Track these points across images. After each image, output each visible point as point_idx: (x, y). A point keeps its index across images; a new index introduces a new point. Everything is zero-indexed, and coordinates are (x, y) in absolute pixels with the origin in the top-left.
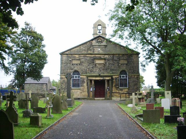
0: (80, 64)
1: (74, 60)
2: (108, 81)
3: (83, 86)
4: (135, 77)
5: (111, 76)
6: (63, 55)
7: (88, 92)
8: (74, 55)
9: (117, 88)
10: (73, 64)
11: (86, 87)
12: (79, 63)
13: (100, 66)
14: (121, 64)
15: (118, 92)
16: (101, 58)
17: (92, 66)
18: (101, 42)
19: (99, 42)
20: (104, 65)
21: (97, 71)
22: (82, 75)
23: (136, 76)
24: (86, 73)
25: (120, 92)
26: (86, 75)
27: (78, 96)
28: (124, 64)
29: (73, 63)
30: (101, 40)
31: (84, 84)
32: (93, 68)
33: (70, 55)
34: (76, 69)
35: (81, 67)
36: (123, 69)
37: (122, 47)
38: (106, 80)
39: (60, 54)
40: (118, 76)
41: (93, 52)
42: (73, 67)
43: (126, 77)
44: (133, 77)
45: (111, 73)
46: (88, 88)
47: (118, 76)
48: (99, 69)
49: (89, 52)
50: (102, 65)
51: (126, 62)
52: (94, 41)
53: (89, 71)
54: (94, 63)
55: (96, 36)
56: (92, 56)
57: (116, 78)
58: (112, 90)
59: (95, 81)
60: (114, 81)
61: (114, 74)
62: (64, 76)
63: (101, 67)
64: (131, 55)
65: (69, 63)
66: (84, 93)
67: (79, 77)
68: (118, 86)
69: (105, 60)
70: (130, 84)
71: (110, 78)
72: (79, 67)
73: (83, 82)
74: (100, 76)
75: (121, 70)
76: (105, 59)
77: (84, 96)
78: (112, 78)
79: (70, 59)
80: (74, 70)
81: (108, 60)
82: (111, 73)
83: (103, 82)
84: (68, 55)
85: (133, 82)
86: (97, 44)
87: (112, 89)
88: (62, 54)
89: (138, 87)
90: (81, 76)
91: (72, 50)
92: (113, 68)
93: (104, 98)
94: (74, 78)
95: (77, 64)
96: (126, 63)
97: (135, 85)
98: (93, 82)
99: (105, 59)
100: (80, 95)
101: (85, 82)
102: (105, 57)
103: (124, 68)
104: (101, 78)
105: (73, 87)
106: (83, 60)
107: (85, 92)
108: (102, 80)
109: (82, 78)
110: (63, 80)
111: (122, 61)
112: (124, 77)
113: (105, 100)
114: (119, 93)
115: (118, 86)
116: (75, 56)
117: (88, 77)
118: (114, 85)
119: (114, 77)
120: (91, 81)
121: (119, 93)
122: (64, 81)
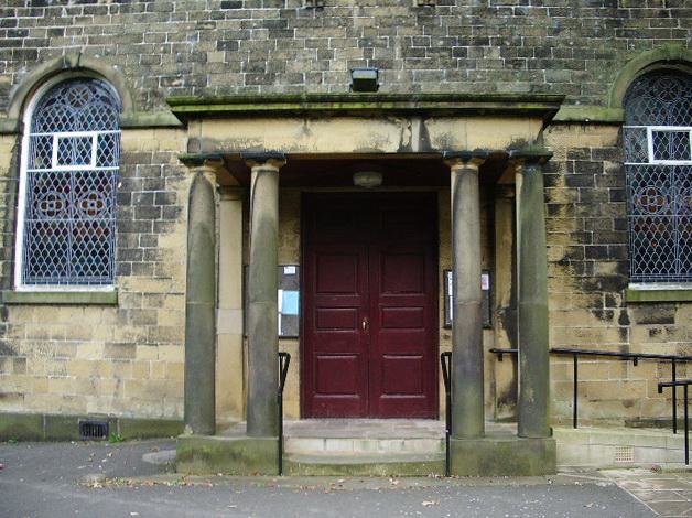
2: (494, 172)
3: (147, 269)
9: (602, 295)
15: (612, 342)
22: (144, 118)
25: (640, 341)
27: (93, 389)
31: (164, 241)
32: (279, 29)
35: (137, 27)
38: (465, 157)
40: (601, 138)
47: (601, 138)
48: (366, 44)
57: (578, 157)
59: (298, 173)
63: (388, 25)
67: (108, 148)
74: (365, 101)
80: (48, 65)
83: (420, 179)
90: (130, 140)
92: (541, 39)
94: (56, 168)
100: (106, 381)
101: (173, 214)
104: (388, 138)
105: (35, 271)
109: (143, 158)
114: (624, 356)
120: (234, 173)
121: (624, 356)
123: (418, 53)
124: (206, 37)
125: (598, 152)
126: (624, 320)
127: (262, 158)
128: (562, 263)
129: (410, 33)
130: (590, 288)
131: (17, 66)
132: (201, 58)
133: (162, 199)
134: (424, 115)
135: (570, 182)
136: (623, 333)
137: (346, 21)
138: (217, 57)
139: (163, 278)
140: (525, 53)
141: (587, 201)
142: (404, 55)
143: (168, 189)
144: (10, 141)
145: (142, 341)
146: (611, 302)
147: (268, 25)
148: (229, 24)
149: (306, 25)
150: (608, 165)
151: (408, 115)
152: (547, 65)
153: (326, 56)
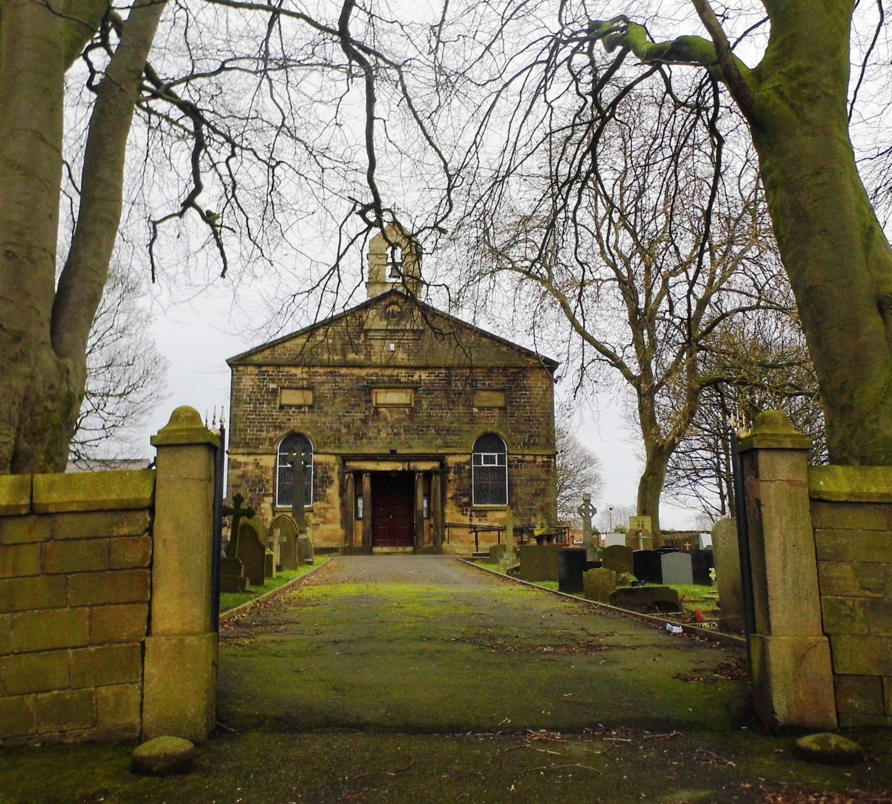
0: (311, 407)
1: (289, 388)
2: (428, 475)
3: (323, 500)
4: (535, 461)
5: (440, 458)
6: (241, 368)
7: (347, 521)
8: (286, 369)
9: (464, 508)
10: (282, 407)
11: (336, 501)
12: (310, 401)
13: (396, 416)
14: (481, 409)
16: (398, 381)
17: (360, 415)
18: (401, 316)
19: (394, 316)
20: (413, 410)
21: (383, 435)
23: (539, 460)
24: (338, 441)
25: (476, 522)
26: (337, 451)
28: (489, 408)
29: (284, 402)
30: (401, 307)
31: (328, 491)
32: (364, 421)
33: (270, 369)
34: (296, 422)
36: (489, 429)
37: (484, 340)
38: (419, 472)
39: (230, 365)
40: (463, 459)
41: (368, 355)
42: (281, 417)
43: (501, 460)
44: (530, 462)
45: (439, 442)
46: (343, 505)
47: (468, 457)
48: (392, 427)
49: (351, 356)
50: (405, 412)
51: (499, 400)
52: (372, 312)
53: (348, 434)
54: (371, 401)
55: (379, 291)
56: (363, 372)
57: (458, 464)
58: (443, 515)
59: (376, 476)
60: (451, 476)
61: (452, 450)
62: (243, 454)
63: (399, 421)
64: (523, 371)
65: (267, 400)
66: (330, 527)
68: (466, 500)
69: (415, 389)
70: (518, 490)
71: (436, 465)
72: (308, 416)
73: (326, 481)
74: (393, 456)
75: (480, 432)
76: (414, 387)
77: (326, 539)
78: (443, 465)
79: (272, 386)
80: (286, 432)
81: (429, 391)
82: (439, 442)
83: (406, 479)
84: (264, 369)
85: (528, 480)
86: (382, 324)
87: (443, 509)
88: (237, 363)
89: (548, 505)
90: (315, 457)
91: (279, 350)
92: (447, 425)
93: (409, 549)
95: (300, 407)
96: (501, 403)
97: (536, 494)
98: (367, 483)
99: (414, 387)
101: (332, 482)
102: (416, 378)
103: (492, 424)
104: (399, 466)
106: (325, 389)
107: (333, 523)
108: (403, 471)
109: (321, 464)
110: (239, 472)
111: (485, 394)
112: (488, 460)
113: (414, 553)
115: (466, 500)
116: (293, 371)
117: (345, 459)
118: (449, 495)
119: (451, 460)
121: (471, 526)
122: (243, 476)
123: (409, 431)
124: (340, 423)
125: (464, 463)
126: (471, 516)
127: (367, 471)
128: (452, 498)
129: (406, 424)
130: (460, 506)
131: (275, 430)
132: (339, 431)
133: (327, 477)
134: (409, 461)
135: (455, 473)
136: (471, 520)
137: (385, 419)
138: (344, 430)
139: (328, 502)
140: (442, 430)
141: (461, 478)
142: (404, 430)
143: (329, 474)
144: (274, 457)
145: (322, 523)
146: (467, 510)
147: (360, 420)
148: (348, 419)
149: (373, 420)
150: (467, 467)
151: (405, 461)
152: (449, 434)
153: (379, 431)
